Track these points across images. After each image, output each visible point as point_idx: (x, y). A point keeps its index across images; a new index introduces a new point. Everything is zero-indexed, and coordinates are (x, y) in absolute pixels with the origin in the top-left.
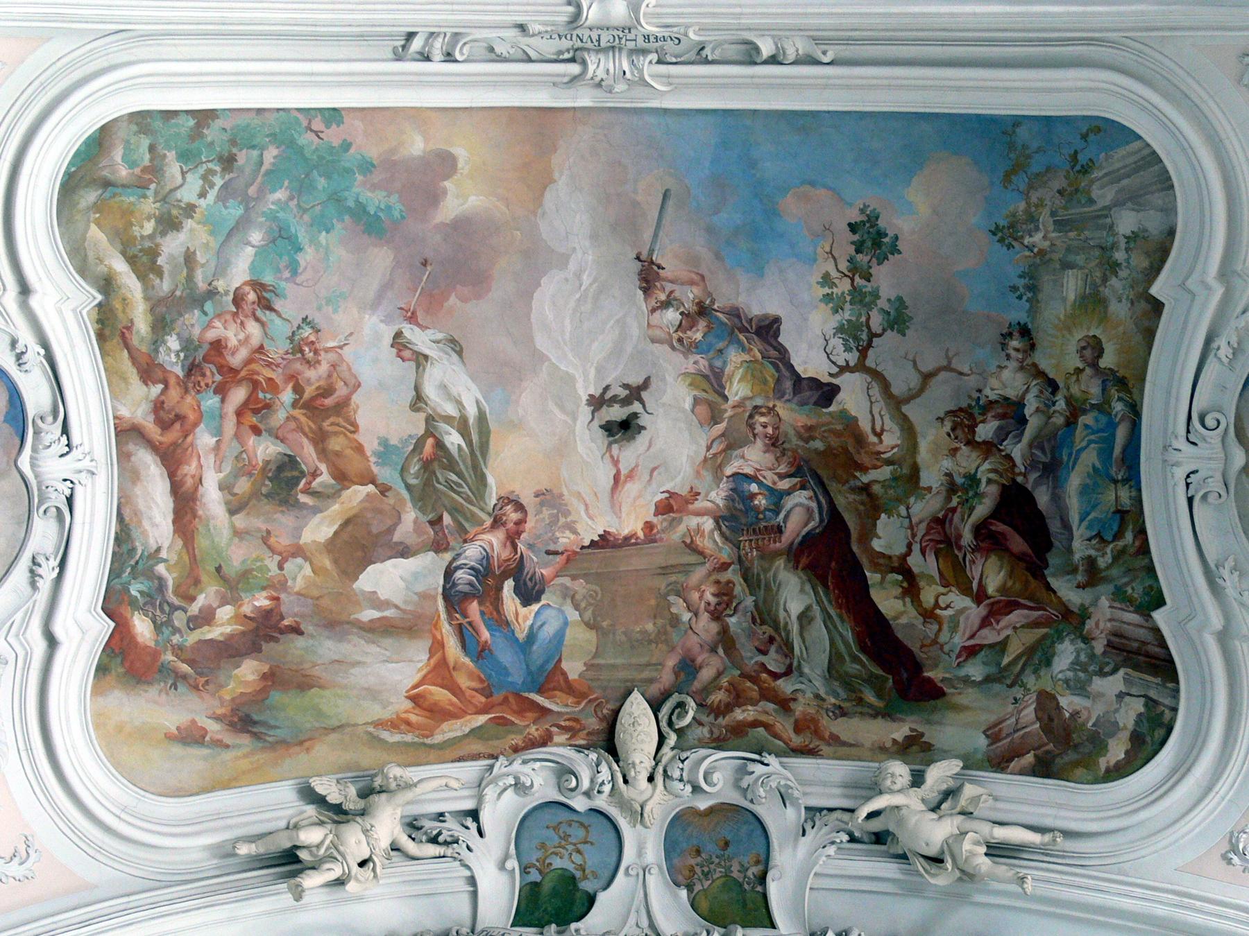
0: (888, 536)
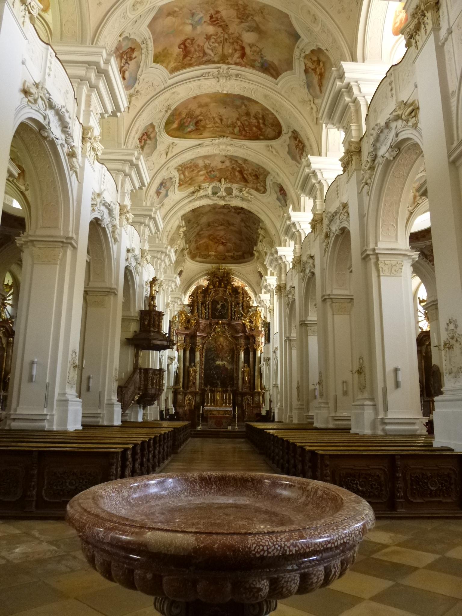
0: (245, 172)
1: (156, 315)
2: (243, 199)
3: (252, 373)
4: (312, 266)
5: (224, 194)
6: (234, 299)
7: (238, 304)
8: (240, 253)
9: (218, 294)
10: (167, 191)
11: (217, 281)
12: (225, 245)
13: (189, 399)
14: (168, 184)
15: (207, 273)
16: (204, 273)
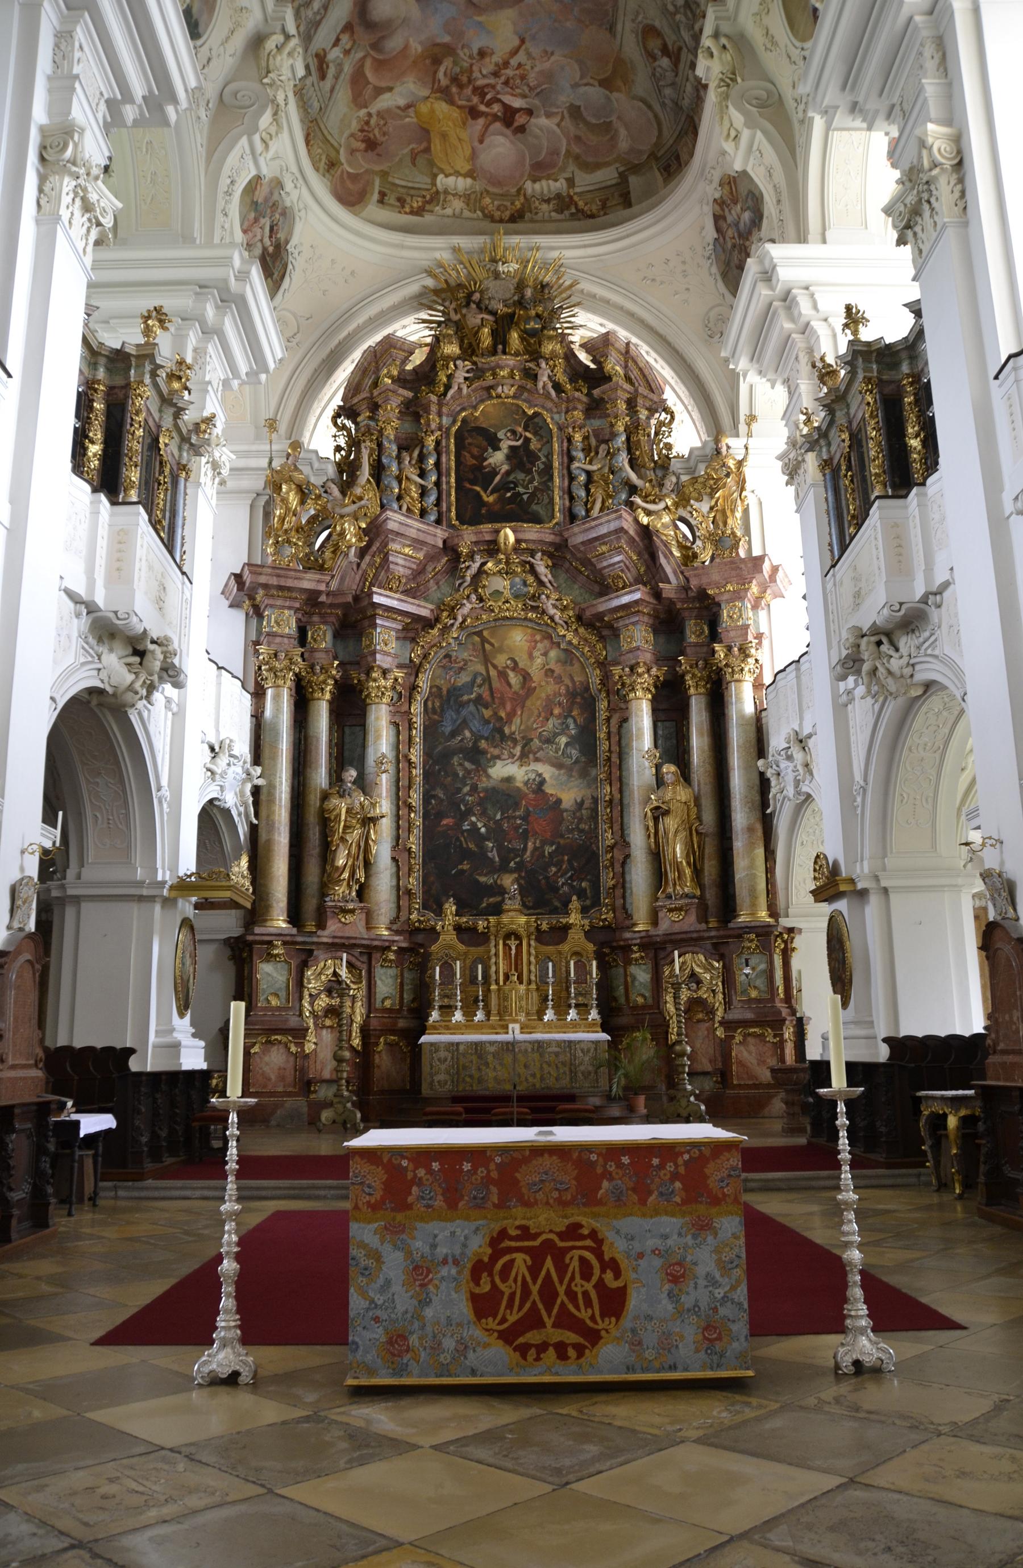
3: (709, 816)
6: (578, 415)
7: (606, 438)
8: (607, 175)
13: (335, 987)
15: (425, 291)
16: (414, 288)
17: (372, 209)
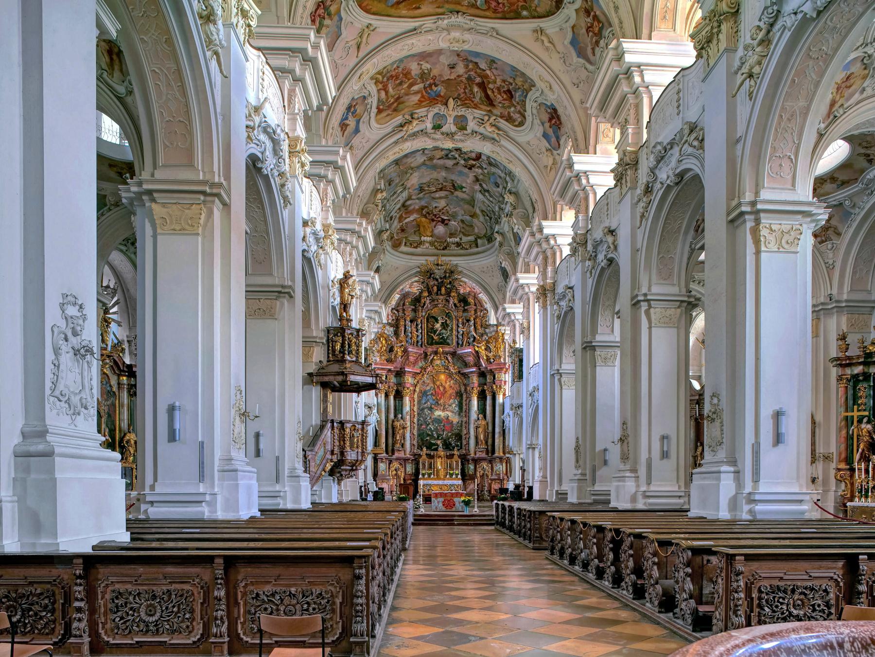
0: (491, 86)
1: (352, 334)
2: (484, 138)
4: (612, 247)
5: (453, 129)
7: (468, 321)
8: (472, 238)
9: (436, 306)
10: (358, 122)
11: (434, 285)
12: (447, 224)
14: (359, 109)
15: (417, 272)
17: (403, 248)
